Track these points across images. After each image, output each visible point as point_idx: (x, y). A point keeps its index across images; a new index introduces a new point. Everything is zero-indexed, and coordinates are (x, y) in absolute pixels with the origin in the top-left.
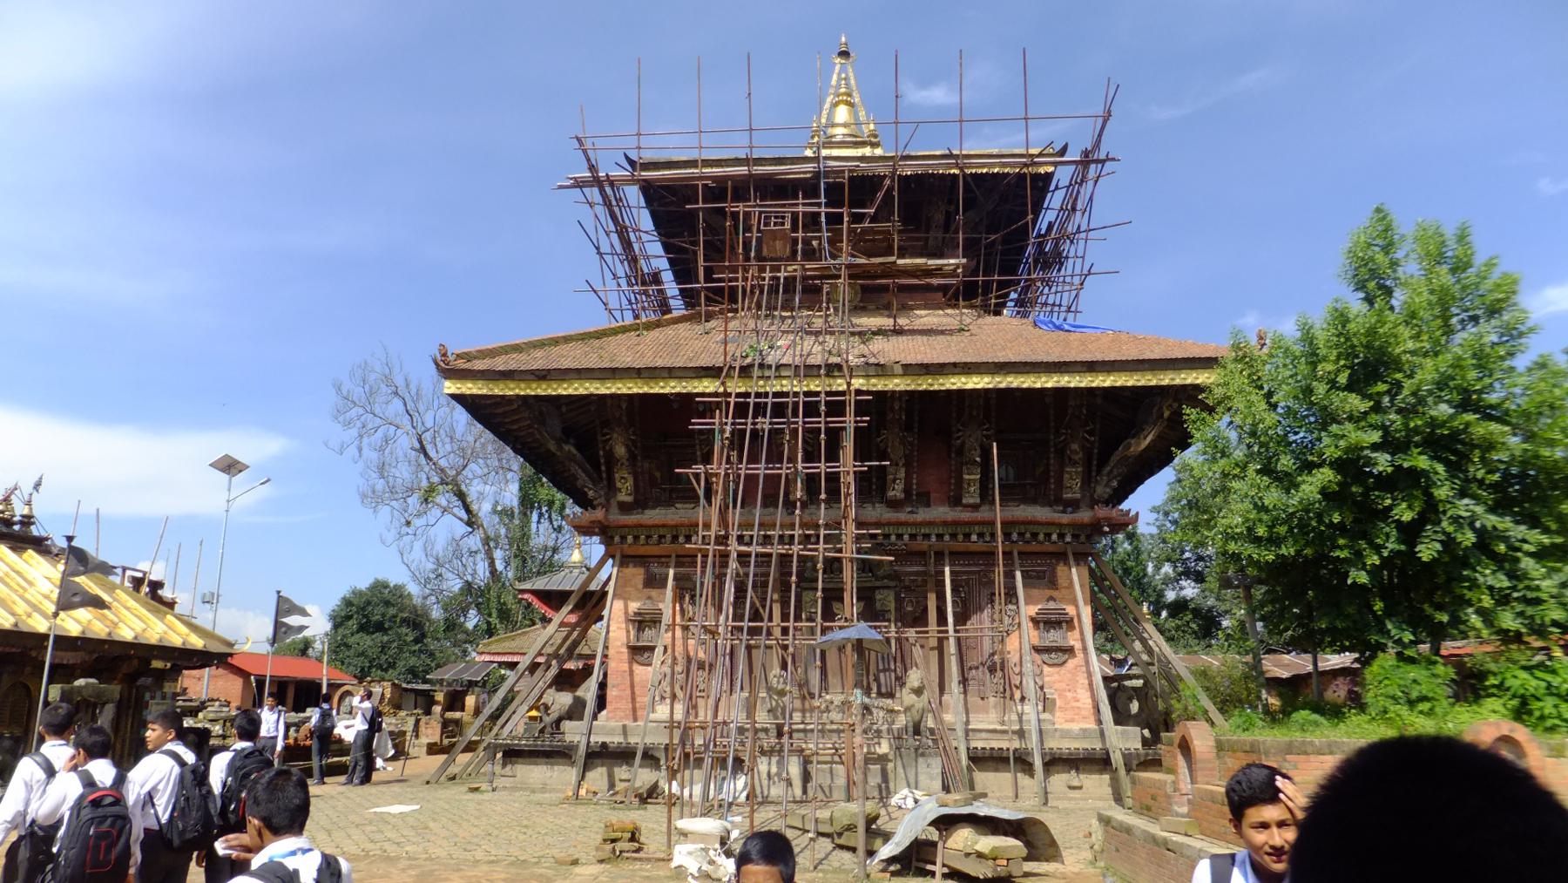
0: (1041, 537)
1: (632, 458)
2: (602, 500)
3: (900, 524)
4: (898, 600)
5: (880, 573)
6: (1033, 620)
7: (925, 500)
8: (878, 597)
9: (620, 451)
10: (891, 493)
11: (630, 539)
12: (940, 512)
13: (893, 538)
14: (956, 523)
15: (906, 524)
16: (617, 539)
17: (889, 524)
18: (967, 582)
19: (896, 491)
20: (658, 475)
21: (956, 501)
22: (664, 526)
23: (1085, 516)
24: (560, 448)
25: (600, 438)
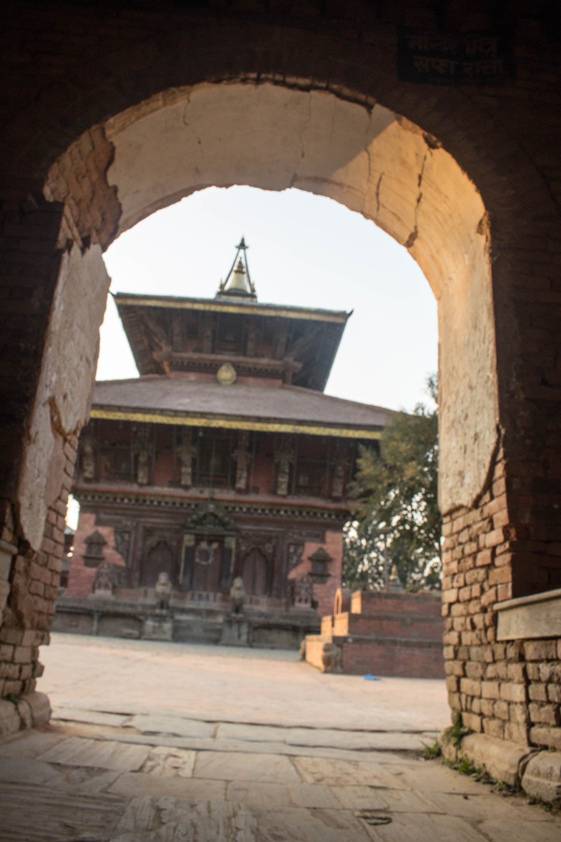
0: (319, 515)
4: (238, 544)
5: (229, 527)
6: (310, 559)
7: (256, 490)
12: (263, 498)
13: (237, 509)
15: (245, 502)
18: (277, 537)
21: (274, 492)
23: (342, 506)
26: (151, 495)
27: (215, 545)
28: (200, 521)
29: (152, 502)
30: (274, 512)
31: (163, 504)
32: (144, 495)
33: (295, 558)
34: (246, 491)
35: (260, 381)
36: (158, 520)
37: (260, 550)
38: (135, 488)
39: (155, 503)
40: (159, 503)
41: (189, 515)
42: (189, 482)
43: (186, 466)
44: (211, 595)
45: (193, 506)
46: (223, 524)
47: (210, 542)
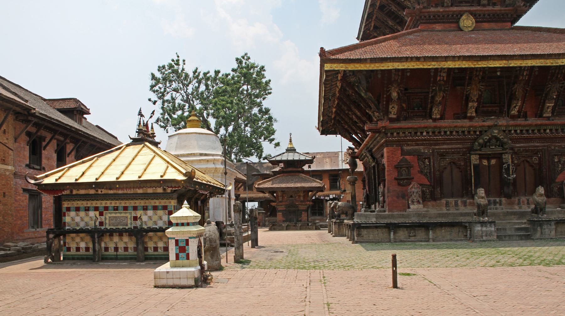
1: (399, 98)
2: (382, 118)
3: (516, 126)
4: (512, 158)
8: (504, 157)
9: (395, 95)
10: (513, 112)
11: (395, 134)
12: (532, 121)
13: (513, 131)
14: (541, 125)
16: (389, 134)
17: (512, 126)
18: (541, 150)
19: (514, 112)
20: (404, 105)
22: (411, 128)
24: (366, 95)
25: (385, 89)
26: (445, 128)
27: (493, 162)
28: (484, 145)
29: (445, 132)
30: (542, 131)
31: (454, 133)
32: (440, 128)
33: (560, 166)
34: (518, 117)
35: (493, 25)
36: (450, 146)
37: (528, 162)
38: (430, 123)
39: (448, 133)
40: (451, 132)
41: (475, 140)
42: (474, 114)
43: (473, 101)
44: (498, 200)
45: (478, 133)
46: (502, 145)
47: (489, 159)
